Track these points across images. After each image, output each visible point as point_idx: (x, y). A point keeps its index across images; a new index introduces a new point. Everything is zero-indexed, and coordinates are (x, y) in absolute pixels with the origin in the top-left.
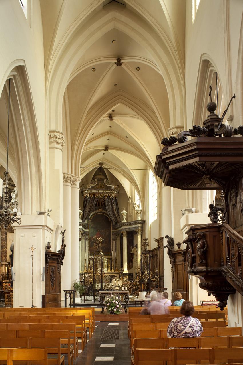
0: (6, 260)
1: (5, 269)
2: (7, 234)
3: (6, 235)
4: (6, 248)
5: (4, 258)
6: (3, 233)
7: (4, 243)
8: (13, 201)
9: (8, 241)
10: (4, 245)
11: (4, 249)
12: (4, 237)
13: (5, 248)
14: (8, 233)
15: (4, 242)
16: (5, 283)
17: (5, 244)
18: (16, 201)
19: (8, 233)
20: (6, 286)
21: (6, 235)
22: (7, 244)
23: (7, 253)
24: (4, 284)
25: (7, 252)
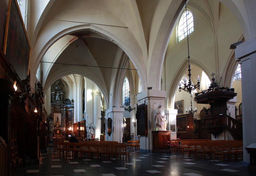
8: (56, 99)
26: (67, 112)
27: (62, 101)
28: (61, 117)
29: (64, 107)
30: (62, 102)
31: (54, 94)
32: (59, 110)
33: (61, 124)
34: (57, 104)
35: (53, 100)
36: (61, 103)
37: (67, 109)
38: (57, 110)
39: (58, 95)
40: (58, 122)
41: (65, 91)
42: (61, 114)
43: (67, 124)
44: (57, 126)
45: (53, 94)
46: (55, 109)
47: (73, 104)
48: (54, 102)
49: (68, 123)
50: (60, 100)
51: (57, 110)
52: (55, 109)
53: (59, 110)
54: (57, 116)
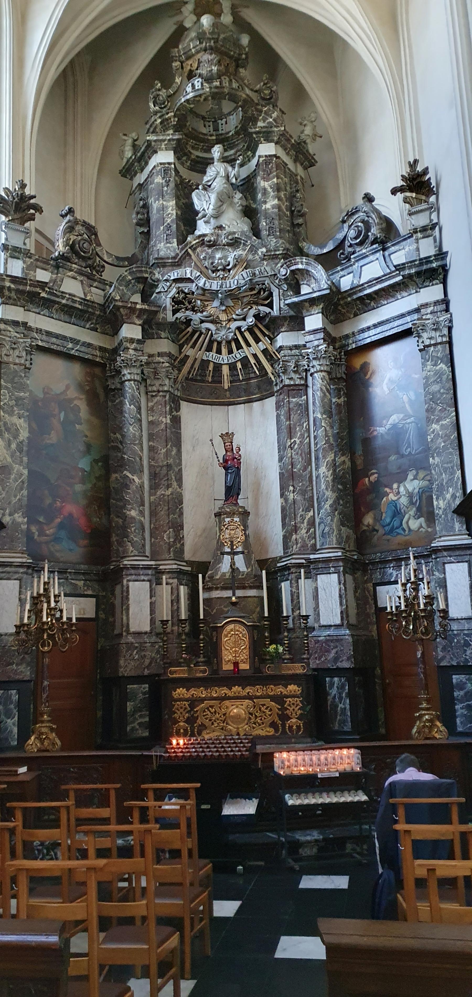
0: (181, 551)
1: (176, 601)
2: (178, 409)
3: (174, 413)
4: (180, 480)
5: (168, 536)
6: (158, 398)
7: (167, 455)
8: (203, 228)
9: (186, 447)
10: (169, 466)
11: (168, 487)
12: (167, 420)
13: (175, 484)
14: (183, 404)
15: (164, 451)
16: (187, 683)
17: (171, 461)
18: (220, 227)
19: (183, 404)
20: (194, 702)
21: (174, 413)
22: (180, 464)
23: (181, 514)
24: (180, 692)
25: (184, 505)
26: (358, 363)
27: (273, 242)
28: (282, 448)
29: (305, 289)
30: (271, 257)
31: (165, 169)
32: (238, 355)
33: (286, 539)
34: (215, 286)
35: (161, 246)
36: (267, 268)
37: (347, 328)
38: (212, 356)
39: (218, 185)
40: (245, 514)
41: (308, 130)
42: (278, 407)
43: (369, 520)
44: (225, 566)
45: (158, 180)
46: (189, 351)
47: (422, 220)
48: (178, 263)
49: (373, 506)
50: (256, 232)
51: (212, 356)
52: (189, 351)
53: (238, 355)
54: (227, 437)
